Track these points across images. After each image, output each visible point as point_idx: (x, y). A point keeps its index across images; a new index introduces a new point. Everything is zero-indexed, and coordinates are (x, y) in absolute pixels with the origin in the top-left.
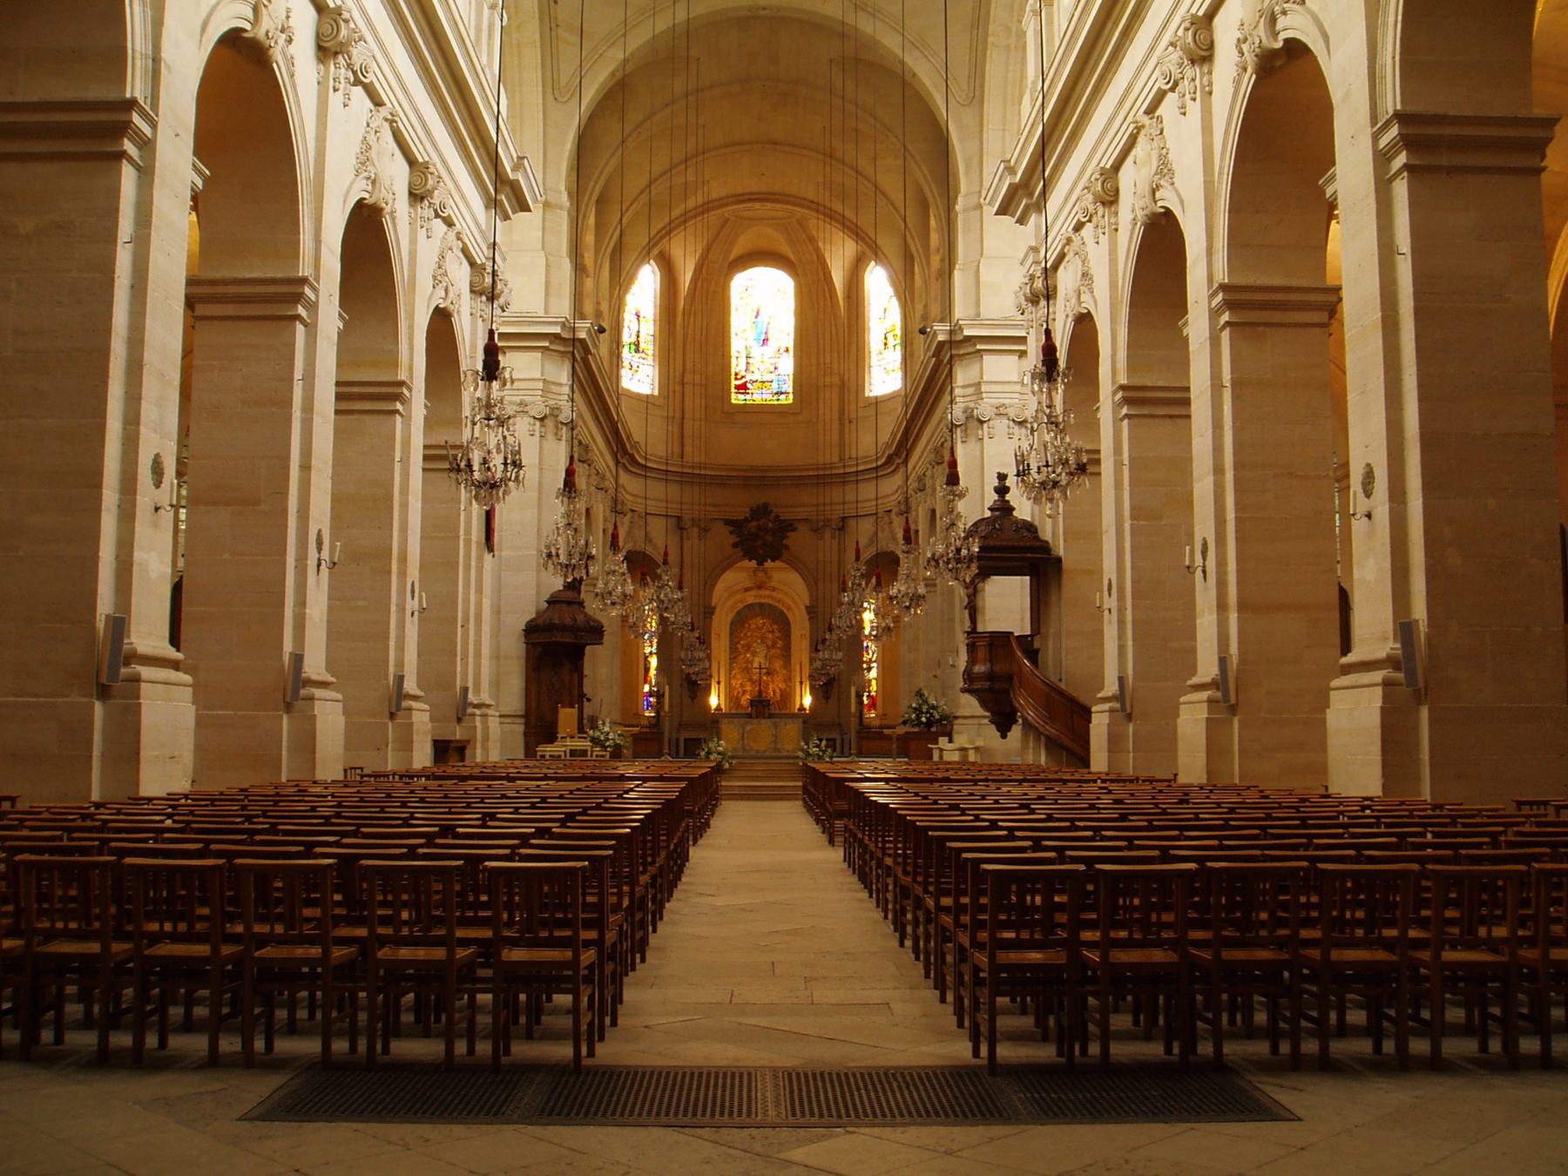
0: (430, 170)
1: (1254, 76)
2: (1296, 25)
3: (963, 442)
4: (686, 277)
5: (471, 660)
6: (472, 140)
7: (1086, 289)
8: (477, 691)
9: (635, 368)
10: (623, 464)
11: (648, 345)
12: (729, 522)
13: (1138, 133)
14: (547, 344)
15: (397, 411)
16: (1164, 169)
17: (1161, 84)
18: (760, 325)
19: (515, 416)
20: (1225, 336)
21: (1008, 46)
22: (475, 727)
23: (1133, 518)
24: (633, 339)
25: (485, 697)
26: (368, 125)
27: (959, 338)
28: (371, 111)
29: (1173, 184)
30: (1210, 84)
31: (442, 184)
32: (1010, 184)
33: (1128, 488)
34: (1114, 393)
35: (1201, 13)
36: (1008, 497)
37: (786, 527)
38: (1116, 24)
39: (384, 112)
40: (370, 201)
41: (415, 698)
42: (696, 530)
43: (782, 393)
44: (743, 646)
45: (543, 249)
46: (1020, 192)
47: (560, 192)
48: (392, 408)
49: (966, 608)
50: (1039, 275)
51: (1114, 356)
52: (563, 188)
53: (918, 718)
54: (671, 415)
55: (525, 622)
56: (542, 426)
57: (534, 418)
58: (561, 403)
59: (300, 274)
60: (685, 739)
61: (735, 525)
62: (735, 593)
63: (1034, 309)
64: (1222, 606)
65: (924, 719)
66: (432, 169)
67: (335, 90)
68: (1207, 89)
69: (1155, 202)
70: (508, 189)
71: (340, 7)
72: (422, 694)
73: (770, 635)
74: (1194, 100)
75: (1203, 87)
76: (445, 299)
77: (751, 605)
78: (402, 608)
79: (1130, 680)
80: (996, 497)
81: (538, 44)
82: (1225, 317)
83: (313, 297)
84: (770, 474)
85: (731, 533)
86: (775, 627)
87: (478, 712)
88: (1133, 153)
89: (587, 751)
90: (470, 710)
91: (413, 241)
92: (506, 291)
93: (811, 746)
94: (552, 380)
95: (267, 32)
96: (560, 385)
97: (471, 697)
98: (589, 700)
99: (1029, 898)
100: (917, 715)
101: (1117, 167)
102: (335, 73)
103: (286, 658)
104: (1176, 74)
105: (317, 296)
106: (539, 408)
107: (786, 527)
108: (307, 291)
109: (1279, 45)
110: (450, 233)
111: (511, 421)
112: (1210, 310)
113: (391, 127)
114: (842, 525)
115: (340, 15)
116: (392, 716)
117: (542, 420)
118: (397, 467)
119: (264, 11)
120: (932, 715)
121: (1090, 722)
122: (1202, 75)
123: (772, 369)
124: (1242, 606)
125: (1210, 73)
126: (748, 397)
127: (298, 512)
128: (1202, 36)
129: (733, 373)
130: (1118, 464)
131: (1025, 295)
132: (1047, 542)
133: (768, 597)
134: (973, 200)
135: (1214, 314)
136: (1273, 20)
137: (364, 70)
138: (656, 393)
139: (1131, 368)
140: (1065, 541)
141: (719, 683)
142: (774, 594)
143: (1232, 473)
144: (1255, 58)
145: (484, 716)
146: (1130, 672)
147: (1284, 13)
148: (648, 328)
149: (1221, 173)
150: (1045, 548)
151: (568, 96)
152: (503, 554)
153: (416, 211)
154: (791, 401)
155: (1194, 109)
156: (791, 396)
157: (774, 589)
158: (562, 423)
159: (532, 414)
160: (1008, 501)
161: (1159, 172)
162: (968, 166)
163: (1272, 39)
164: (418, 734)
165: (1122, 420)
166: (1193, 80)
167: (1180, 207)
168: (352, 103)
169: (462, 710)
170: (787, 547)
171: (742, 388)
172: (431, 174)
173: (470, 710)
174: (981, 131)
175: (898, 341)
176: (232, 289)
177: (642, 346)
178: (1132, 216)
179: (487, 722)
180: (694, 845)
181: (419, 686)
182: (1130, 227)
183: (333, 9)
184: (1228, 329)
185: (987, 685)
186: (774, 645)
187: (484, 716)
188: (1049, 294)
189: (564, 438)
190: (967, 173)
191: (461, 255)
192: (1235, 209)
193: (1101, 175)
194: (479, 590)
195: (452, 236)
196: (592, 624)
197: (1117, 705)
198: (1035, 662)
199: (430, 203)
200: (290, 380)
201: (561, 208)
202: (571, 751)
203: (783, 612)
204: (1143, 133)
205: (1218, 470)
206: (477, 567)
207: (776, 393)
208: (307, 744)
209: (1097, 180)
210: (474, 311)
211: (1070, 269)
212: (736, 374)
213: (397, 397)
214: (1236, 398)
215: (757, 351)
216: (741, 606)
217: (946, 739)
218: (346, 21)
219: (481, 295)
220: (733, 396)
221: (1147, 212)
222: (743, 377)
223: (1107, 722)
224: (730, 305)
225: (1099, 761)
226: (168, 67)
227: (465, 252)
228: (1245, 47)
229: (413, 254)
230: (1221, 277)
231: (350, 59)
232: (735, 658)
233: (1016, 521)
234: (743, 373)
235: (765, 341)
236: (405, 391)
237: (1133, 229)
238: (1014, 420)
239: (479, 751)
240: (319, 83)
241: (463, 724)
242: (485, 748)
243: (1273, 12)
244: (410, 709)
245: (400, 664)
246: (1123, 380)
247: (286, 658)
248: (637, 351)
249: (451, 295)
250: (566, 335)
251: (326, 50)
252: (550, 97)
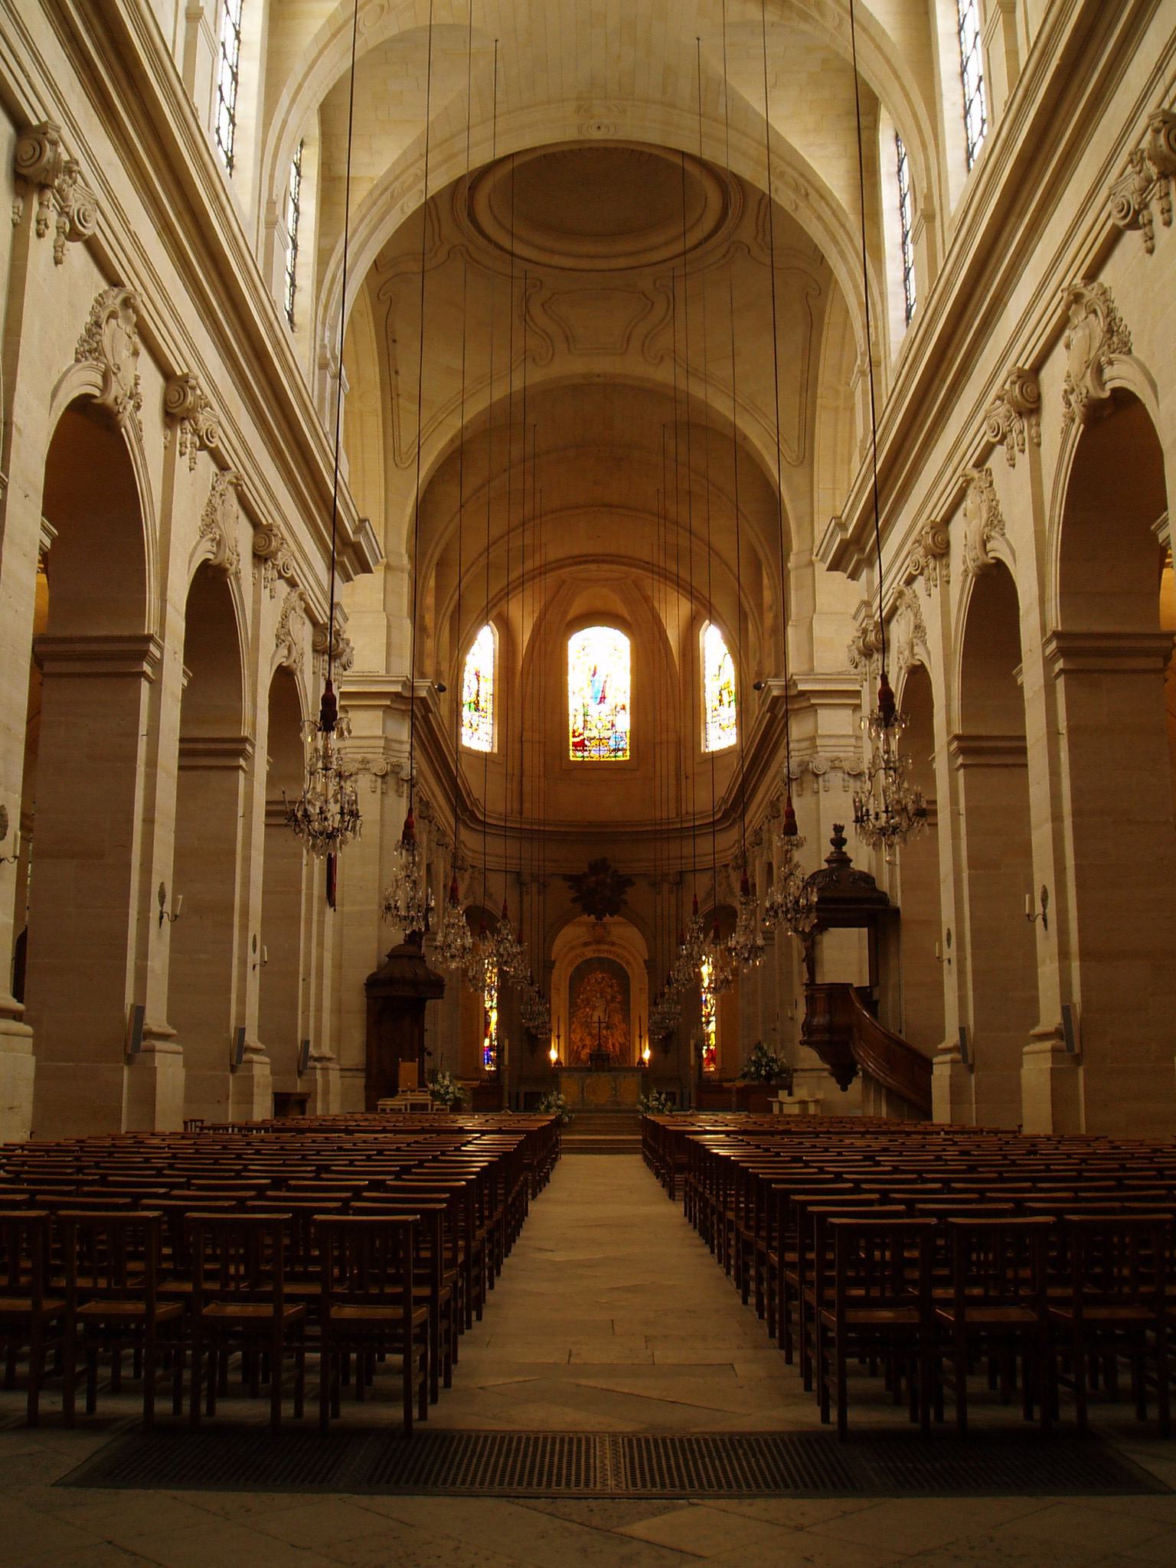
1: (1082, 426)
2: (1123, 375)
3: (799, 795)
4: (524, 637)
5: (312, 1014)
6: (315, 504)
7: (920, 644)
8: (318, 1044)
9: (474, 726)
10: (464, 820)
11: (487, 704)
12: (567, 878)
13: (967, 486)
14: (389, 703)
15: (241, 767)
16: (995, 520)
17: (989, 437)
18: (597, 684)
19: (357, 774)
20: (1060, 683)
21: (837, 408)
22: (316, 1080)
23: (971, 867)
24: (473, 698)
25: (326, 1050)
26: (213, 488)
27: (793, 692)
28: (217, 475)
29: (1003, 535)
30: (1039, 436)
31: (285, 546)
32: (841, 540)
33: (965, 838)
34: (949, 743)
35: (1027, 367)
36: (844, 849)
37: (624, 882)
38: (943, 381)
39: (229, 476)
41: (256, 1051)
42: (534, 888)
43: (619, 750)
44: (583, 1001)
45: (385, 610)
46: (851, 548)
47: (401, 555)
48: (235, 764)
49: (804, 961)
50: (871, 628)
51: (948, 706)
52: (404, 551)
53: (758, 1071)
54: (510, 771)
55: (366, 977)
56: (382, 783)
57: (376, 775)
58: (403, 760)
59: (146, 632)
60: (526, 1094)
61: (574, 880)
62: (572, 948)
63: (867, 663)
64: (1064, 954)
65: (763, 1072)
66: (275, 531)
67: (182, 454)
68: (1035, 440)
69: (987, 554)
70: (350, 551)
71: (187, 374)
72: (263, 1047)
73: (609, 990)
74: (1023, 451)
75: (1031, 439)
77: (590, 959)
78: (243, 962)
79: (972, 1031)
80: (832, 848)
81: (380, 413)
82: (1060, 665)
83: (158, 655)
84: (609, 830)
85: (570, 888)
87: (318, 1065)
88: (963, 506)
89: (427, 1105)
90: (311, 1064)
91: (257, 601)
92: (348, 650)
93: (651, 1099)
94: (394, 738)
95: (116, 399)
96: (401, 742)
97: (313, 1051)
98: (429, 1054)
99: (1115, 1270)
100: (757, 1068)
101: (947, 519)
102: (181, 438)
103: (128, 1011)
104: (1004, 428)
105: (162, 654)
106: (380, 764)
107: (624, 882)
108: (152, 648)
109: (1106, 394)
110: (293, 594)
111: (353, 778)
112: (1045, 659)
113: (236, 491)
114: (680, 880)
115: (187, 382)
116: (233, 1069)
117: (383, 777)
118: (240, 822)
120: (771, 1067)
121: (932, 1073)
122: (1030, 427)
123: (609, 726)
124: (1085, 955)
125: (1038, 425)
126: (586, 754)
127: (141, 865)
128: (1029, 389)
129: (571, 731)
130: (955, 815)
131: (858, 649)
132: (885, 894)
134: (805, 559)
135: (1048, 662)
136: (1099, 370)
137: (210, 435)
138: (496, 750)
139: (965, 719)
140: (902, 892)
141: (558, 1037)
142: (613, 949)
143: (1071, 820)
144: (1082, 409)
145: (325, 1069)
146: (971, 1023)
147: (1111, 363)
148: (487, 688)
149: (1051, 523)
150: (883, 899)
151: (406, 465)
152: (345, 908)
153: (260, 572)
154: (628, 758)
155: (1023, 461)
156: (628, 753)
157: (613, 944)
158: (403, 780)
159: (374, 770)
160: (845, 853)
161: (990, 524)
162: (799, 526)
163: (1098, 389)
164: (258, 1086)
165: (958, 769)
166: (1021, 432)
167: (1011, 558)
168: (199, 467)
169: (303, 1062)
170: (626, 903)
171: (581, 745)
172: (275, 536)
173: (311, 1064)
174: (812, 491)
175: (733, 698)
176: (80, 647)
177: (482, 705)
178: (962, 568)
179: (328, 1075)
180: (533, 1199)
181: (261, 1038)
182: (961, 578)
183: (180, 377)
184: (1063, 676)
185: (826, 1037)
186: (613, 998)
187: (325, 1069)
188: (884, 647)
189: (405, 795)
190: (798, 532)
191: (304, 616)
192: (1066, 557)
193: (932, 528)
194: (321, 944)
195: (294, 596)
196: (432, 978)
197: (958, 1056)
198: (874, 1013)
199: (273, 565)
200: (135, 735)
201: (402, 571)
202: (411, 1104)
204: (972, 485)
205: (1057, 817)
206: (319, 921)
207: (614, 750)
208: (146, 1095)
209: (927, 533)
210: (316, 670)
211: (903, 622)
212: (574, 732)
213: (242, 753)
214: (1072, 746)
215: (594, 709)
216: (580, 960)
217: (786, 1092)
218: (193, 388)
219: (323, 654)
220: (571, 753)
221: (979, 563)
222: (580, 735)
223: (949, 1073)
224: (567, 664)
225: (941, 1112)
226: (19, 430)
227: (308, 611)
228: (1072, 398)
229: (256, 614)
230: (1054, 625)
231: (196, 425)
232: (574, 1012)
233: (854, 873)
234: (581, 731)
235: (603, 699)
236: (249, 748)
237: (964, 581)
238: (849, 774)
239: (319, 1105)
240: (165, 448)
241: (304, 1078)
242: (326, 1102)
243: (1099, 363)
244: (251, 1062)
245: (241, 1017)
246: (958, 730)
247: (128, 1011)
248: (477, 709)
249: (294, 654)
250: (407, 694)
251: (173, 416)
252: (391, 463)
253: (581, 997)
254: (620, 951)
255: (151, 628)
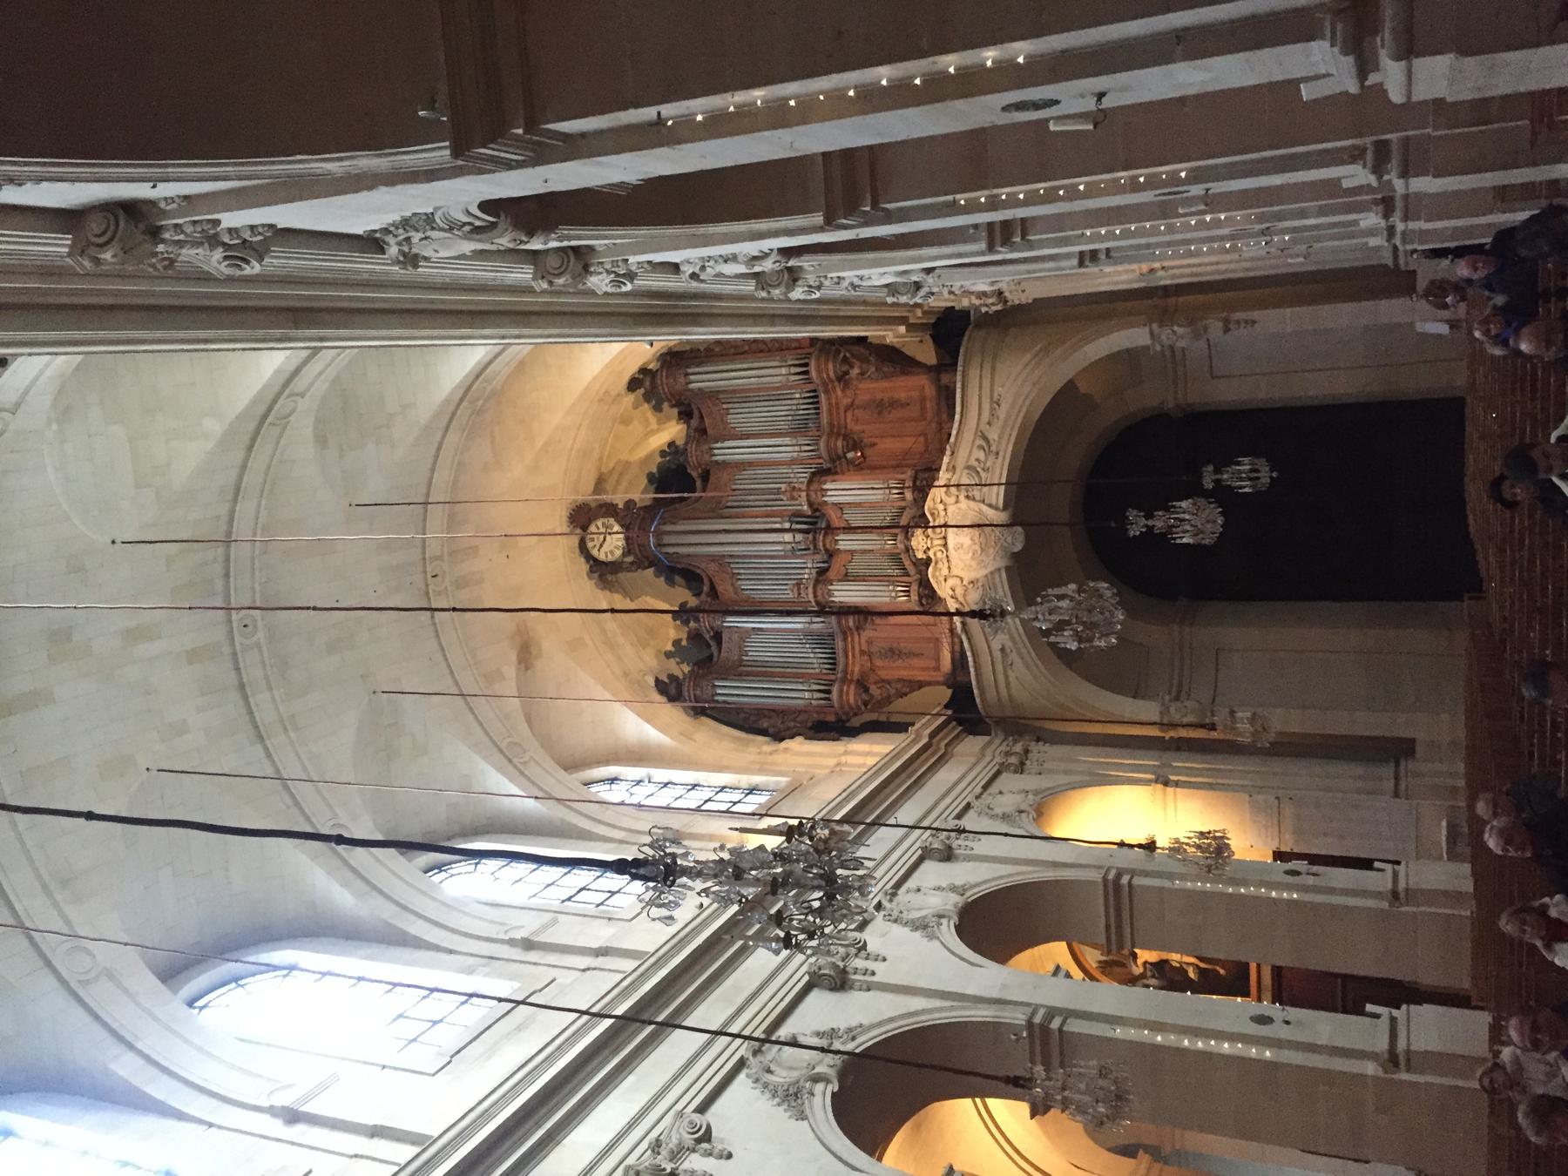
0: (928, 844)
26: (896, 921)
39: (885, 903)
40: (955, 919)
67: (873, 973)
76: (1028, 813)
105: (1042, 1006)
119: (816, 1071)
255: (1018, 1017)
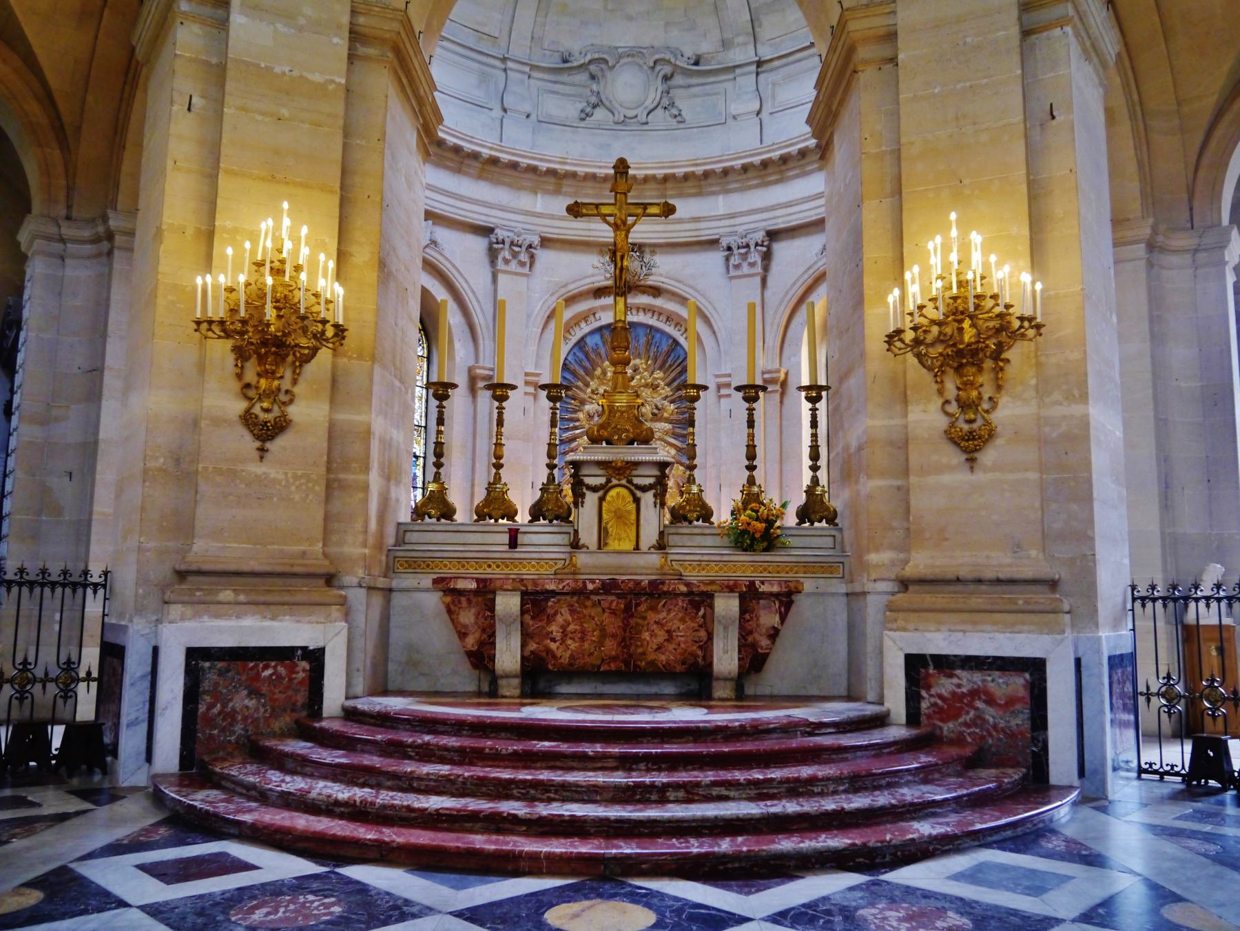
60: (194, 655)
62: (571, 300)
86: (659, 374)
133: (646, 309)
142: (659, 302)
157: (656, 291)
203: (675, 342)
216: (585, 328)
253: (587, 407)
254: (672, 306)
